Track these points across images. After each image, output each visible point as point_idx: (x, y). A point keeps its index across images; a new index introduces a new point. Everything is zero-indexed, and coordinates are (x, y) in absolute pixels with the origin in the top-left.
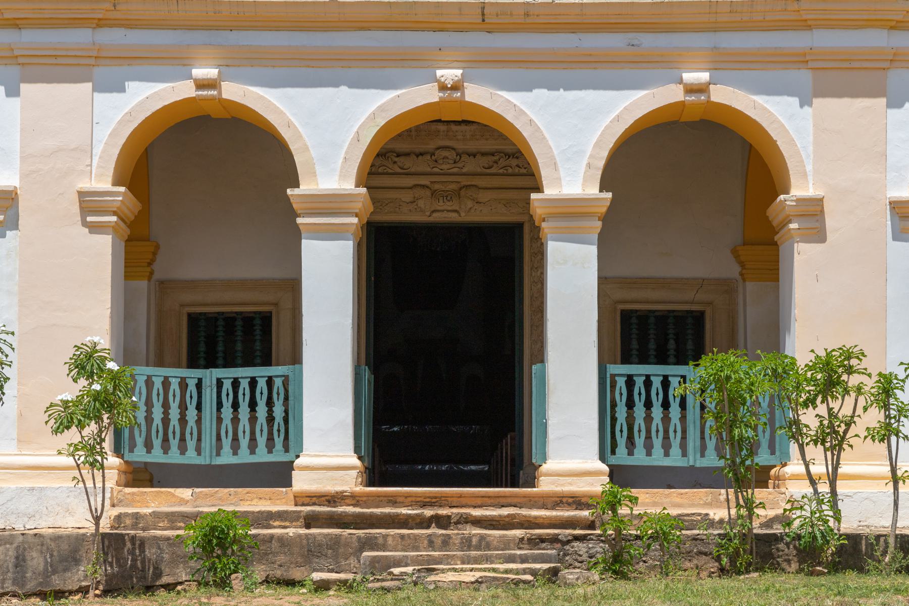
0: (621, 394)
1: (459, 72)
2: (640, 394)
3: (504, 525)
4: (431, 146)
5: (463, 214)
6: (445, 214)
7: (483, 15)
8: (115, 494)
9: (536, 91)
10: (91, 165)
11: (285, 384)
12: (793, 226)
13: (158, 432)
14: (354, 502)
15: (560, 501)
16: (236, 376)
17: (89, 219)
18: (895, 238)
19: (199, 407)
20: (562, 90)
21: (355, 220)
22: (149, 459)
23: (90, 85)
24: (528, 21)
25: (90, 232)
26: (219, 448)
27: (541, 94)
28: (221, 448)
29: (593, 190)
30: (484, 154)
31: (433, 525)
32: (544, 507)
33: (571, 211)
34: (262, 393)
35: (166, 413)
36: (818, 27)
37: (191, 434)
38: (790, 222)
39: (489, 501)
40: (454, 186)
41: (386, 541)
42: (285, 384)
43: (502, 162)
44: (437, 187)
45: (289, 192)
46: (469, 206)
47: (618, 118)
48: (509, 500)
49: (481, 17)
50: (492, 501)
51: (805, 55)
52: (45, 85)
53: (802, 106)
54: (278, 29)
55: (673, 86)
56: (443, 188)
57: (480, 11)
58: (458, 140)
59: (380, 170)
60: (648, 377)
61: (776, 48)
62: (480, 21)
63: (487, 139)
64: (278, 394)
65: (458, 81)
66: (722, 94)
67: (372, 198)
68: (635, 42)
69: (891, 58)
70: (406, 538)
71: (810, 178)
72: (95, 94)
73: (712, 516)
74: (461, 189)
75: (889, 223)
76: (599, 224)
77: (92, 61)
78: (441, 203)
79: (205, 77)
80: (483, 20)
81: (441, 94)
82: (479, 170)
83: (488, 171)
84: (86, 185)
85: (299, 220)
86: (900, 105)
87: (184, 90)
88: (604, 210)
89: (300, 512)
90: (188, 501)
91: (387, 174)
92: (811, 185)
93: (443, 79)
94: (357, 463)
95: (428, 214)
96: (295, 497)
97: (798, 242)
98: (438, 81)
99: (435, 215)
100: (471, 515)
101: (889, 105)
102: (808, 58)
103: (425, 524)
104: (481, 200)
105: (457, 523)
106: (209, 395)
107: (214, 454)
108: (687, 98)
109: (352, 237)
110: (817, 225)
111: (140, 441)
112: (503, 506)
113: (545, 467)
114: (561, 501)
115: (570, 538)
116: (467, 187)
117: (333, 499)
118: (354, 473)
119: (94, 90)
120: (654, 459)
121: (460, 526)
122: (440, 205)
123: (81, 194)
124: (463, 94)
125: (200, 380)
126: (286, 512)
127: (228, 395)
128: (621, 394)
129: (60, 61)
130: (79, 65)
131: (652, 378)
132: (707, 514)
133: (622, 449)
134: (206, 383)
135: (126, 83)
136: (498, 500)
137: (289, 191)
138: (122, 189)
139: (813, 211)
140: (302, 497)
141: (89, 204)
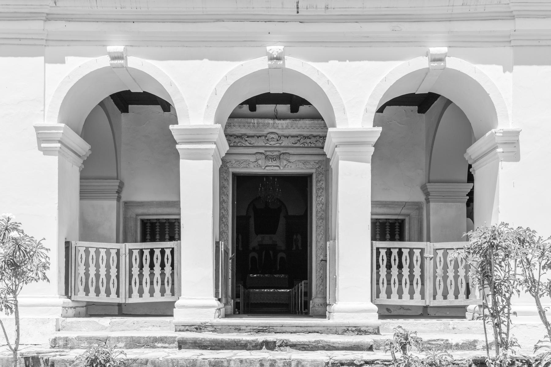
0: (383, 260)
1: (282, 48)
2: (395, 260)
3: (312, 347)
4: (265, 132)
5: (282, 168)
6: (272, 168)
7: (298, 8)
8: (60, 323)
9: (331, 62)
10: (44, 110)
11: (172, 252)
12: (499, 150)
13: (92, 282)
14: (213, 329)
15: (346, 330)
16: (141, 248)
17: (43, 145)
19: (118, 267)
20: (348, 61)
21: (214, 146)
22: (87, 299)
23: (42, 58)
24: (327, 14)
25: (44, 154)
26: (131, 292)
27: (334, 64)
28: (132, 293)
29: (369, 126)
30: (292, 137)
31: (264, 347)
32: (337, 333)
33: (353, 141)
34: (157, 259)
35: (98, 270)
36: (520, 16)
37: (113, 284)
38: (496, 147)
39: (301, 329)
40: (277, 153)
41: (229, 364)
42: (172, 252)
43: (302, 141)
44: (268, 153)
45: (171, 127)
46: (285, 164)
48: (314, 329)
49: (296, 10)
50: (303, 329)
52: (13, 58)
53: (504, 72)
54: (164, 22)
56: (271, 154)
57: (296, 4)
58: (279, 129)
59: (239, 145)
60: (400, 249)
62: (295, 13)
63: (294, 128)
64: (168, 259)
65: (281, 53)
66: (454, 63)
67: (228, 136)
70: (244, 362)
72: (46, 64)
73: (450, 342)
74: (280, 155)
76: (373, 149)
77: (44, 42)
78: (270, 162)
79: (115, 51)
80: (298, 12)
81: (270, 62)
82: (290, 145)
83: (295, 145)
84: (41, 123)
85: (178, 147)
87: (104, 62)
88: (375, 140)
89: (175, 337)
90: (107, 327)
91: (242, 146)
93: (271, 52)
94: (215, 303)
95: (263, 168)
96: (176, 326)
98: (267, 54)
99: (267, 168)
100: (290, 341)
102: (511, 38)
103: (259, 347)
104: (290, 161)
105: (280, 346)
106: (124, 260)
107: (128, 296)
108: (432, 64)
109: (212, 158)
111: (81, 288)
112: (310, 332)
113: (335, 307)
114: (348, 329)
115: (362, 362)
116: (283, 153)
117: (199, 328)
118: (214, 310)
119: (46, 62)
120: (404, 301)
121: (282, 348)
122: (270, 163)
123: (37, 128)
124: (284, 63)
125: (118, 250)
126: (166, 337)
127: (136, 259)
128: (383, 260)
129: (23, 42)
130: (35, 45)
131: (403, 250)
132: (447, 340)
134: (122, 252)
135: (66, 58)
136: (306, 328)
137: (171, 127)
138: (63, 125)
140: (179, 326)
141: (43, 136)
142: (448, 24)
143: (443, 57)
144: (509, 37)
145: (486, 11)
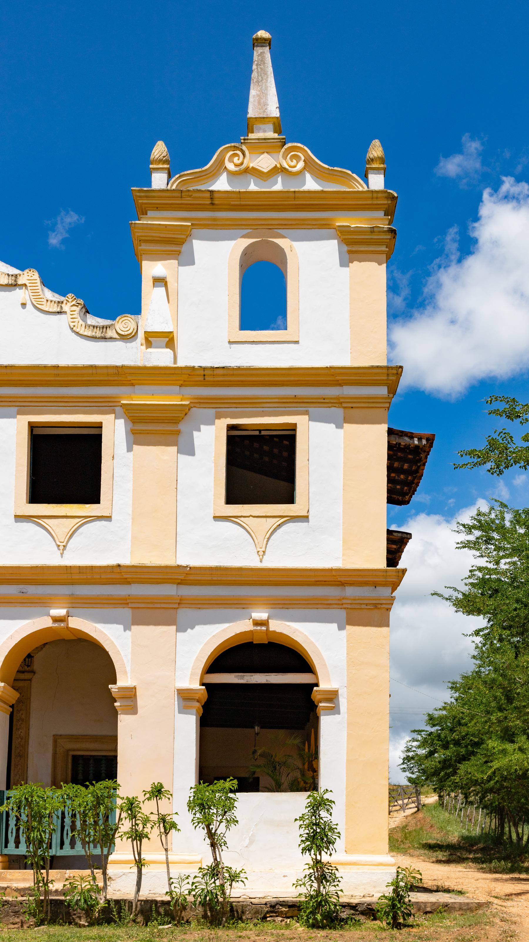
36: (134, 582)
47: (11, 637)
51: (126, 600)
53: (125, 630)
55: (46, 618)
61: (108, 595)
66: (76, 623)
68: (24, 591)
69: (178, 601)
71: (129, 675)
75: (176, 703)
86: (185, 631)
92: (129, 679)
97: (120, 714)
101: (177, 631)
102: (128, 601)
110: (132, 704)
133: (12, 844)
139: (130, 694)
142: (70, 587)
143: (63, 618)
144: (126, 600)
145: (102, 577)
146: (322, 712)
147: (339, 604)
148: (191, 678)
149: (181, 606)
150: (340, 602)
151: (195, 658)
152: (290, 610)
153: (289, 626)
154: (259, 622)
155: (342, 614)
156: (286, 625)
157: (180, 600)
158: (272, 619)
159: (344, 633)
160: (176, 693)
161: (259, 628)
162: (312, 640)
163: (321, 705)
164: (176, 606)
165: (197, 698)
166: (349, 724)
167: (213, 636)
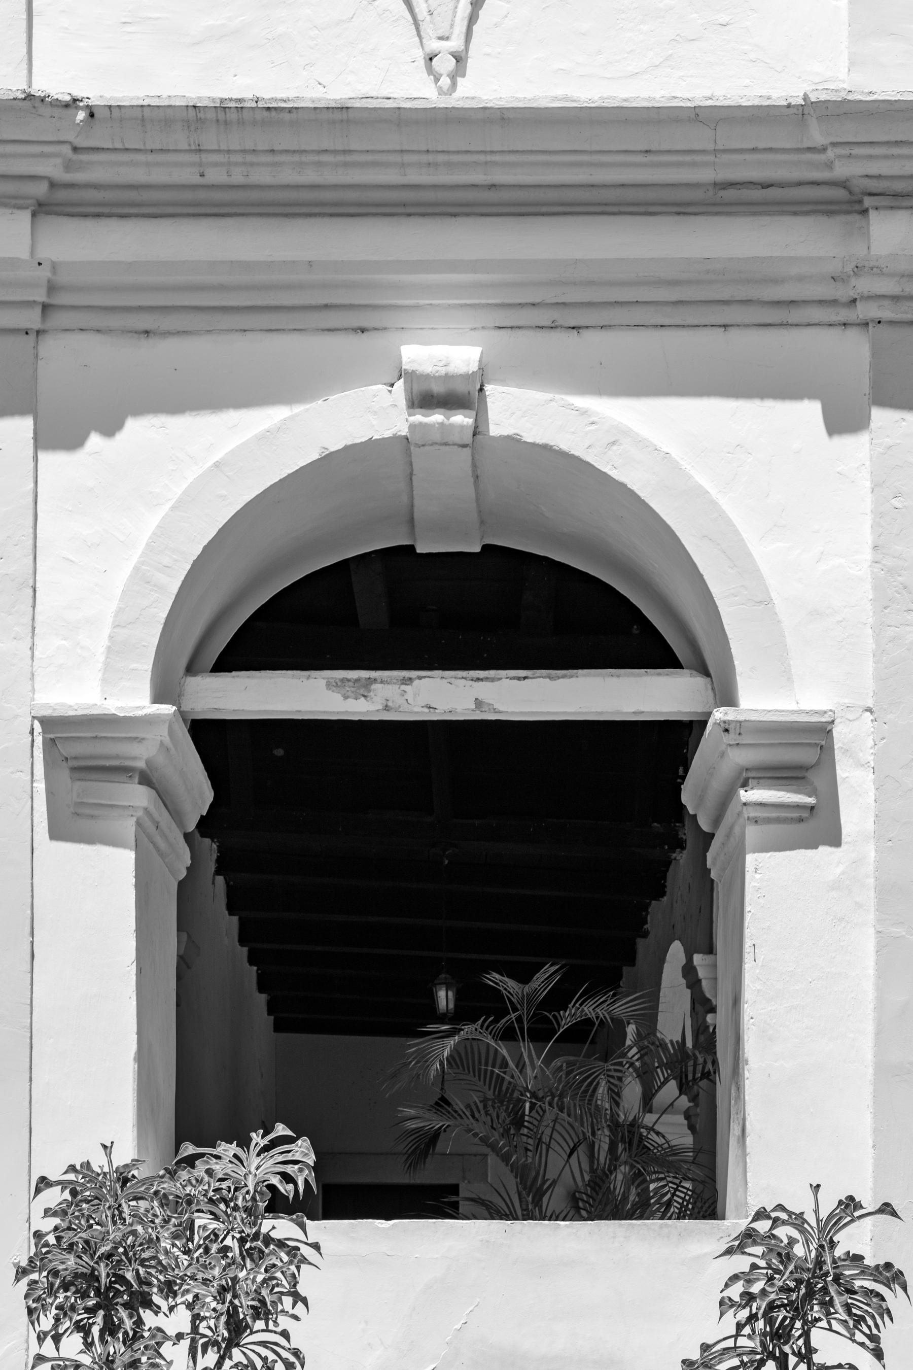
18: (56, 834)
69: (41, 296)
86: (74, 442)
146: (752, 833)
147: (834, 303)
148: (107, 667)
149: (59, 319)
150: (842, 293)
151: (126, 570)
152: (591, 337)
153: (584, 413)
154: (438, 389)
155: (852, 352)
156: (570, 407)
157: (52, 288)
158: (503, 382)
159: (855, 448)
160: (39, 740)
161: (437, 417)
162: (702, 480)
163: (745, 795)
164: (32, 319)
165: (141, 764)
166: (889, 894)
167: (217, 465)
